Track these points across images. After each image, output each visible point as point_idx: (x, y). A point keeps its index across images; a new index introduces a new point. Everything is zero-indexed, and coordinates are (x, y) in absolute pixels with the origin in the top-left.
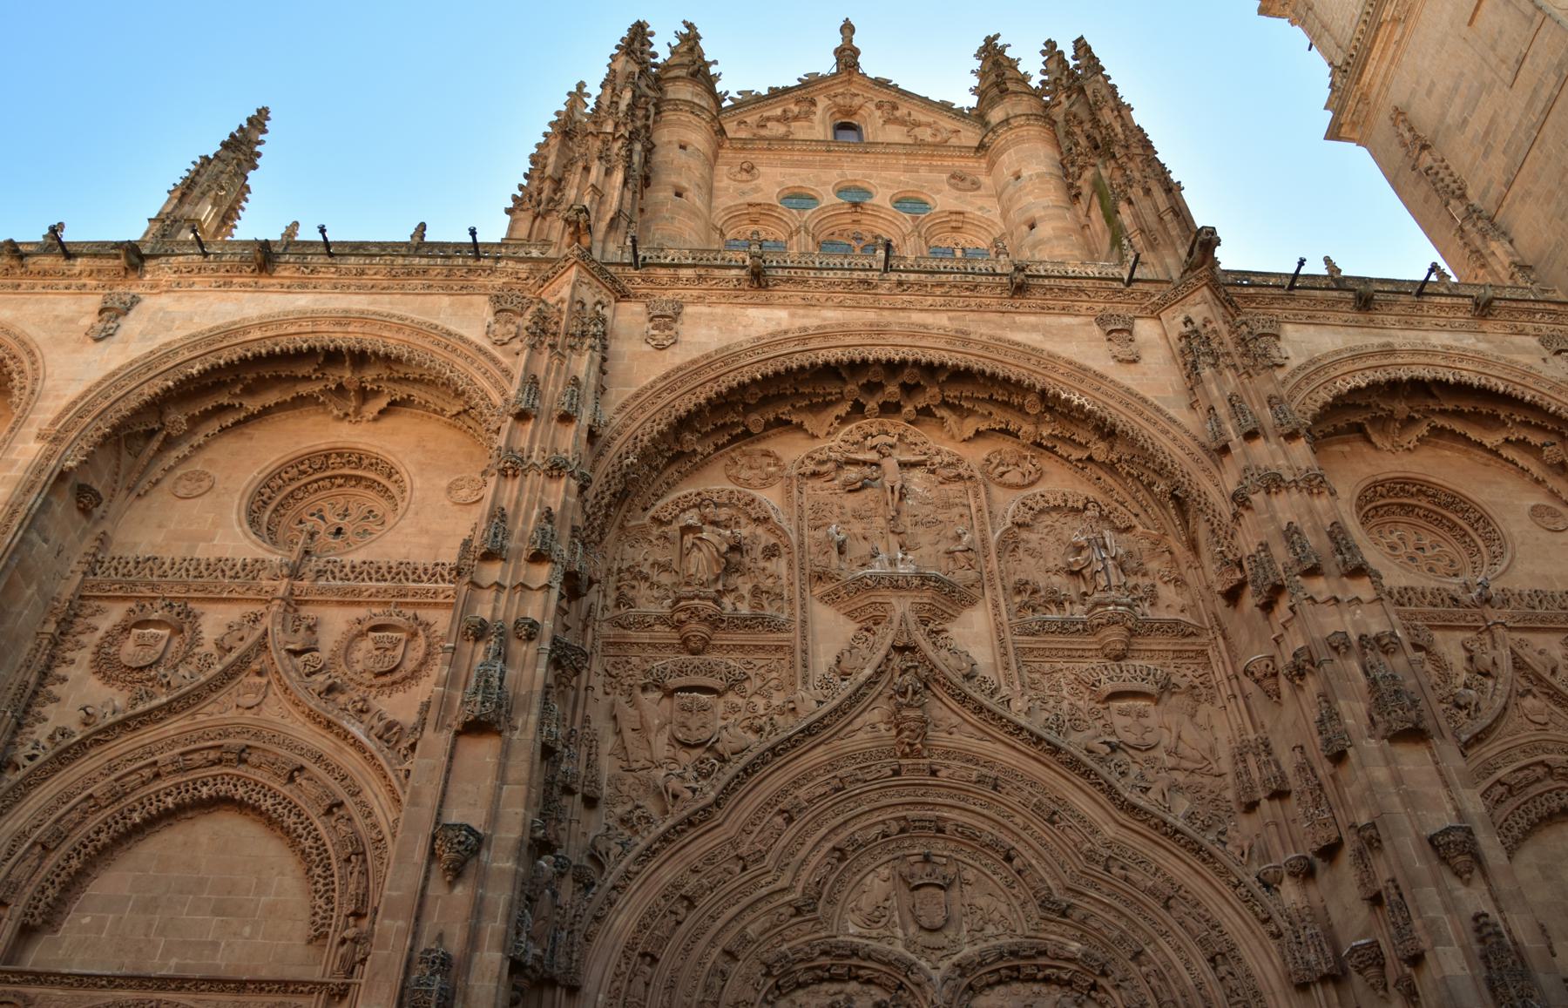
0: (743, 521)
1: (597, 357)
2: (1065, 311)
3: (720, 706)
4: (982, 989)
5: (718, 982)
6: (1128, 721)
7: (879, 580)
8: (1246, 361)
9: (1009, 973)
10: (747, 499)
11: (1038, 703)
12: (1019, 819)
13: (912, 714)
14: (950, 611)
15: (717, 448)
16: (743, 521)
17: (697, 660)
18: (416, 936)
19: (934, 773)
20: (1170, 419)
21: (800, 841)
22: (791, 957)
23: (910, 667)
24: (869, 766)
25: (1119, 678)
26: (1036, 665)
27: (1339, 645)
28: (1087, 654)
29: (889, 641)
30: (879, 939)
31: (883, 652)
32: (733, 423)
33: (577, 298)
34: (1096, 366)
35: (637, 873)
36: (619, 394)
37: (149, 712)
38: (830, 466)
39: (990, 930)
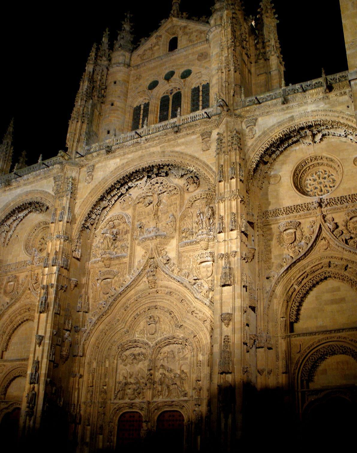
1: (69, 197)
2: (193, 133)
3: (113, 281)
4: (163, 347)
6: (205, 269)
7: (146, 239)
8: (229, 148)
10: (121, 217)
12: (175, 303)
13: (151, 278)
15: (116, 201)
16: (121, 223)
18: (34, 357)
20: (214, 172)
22: (123, 344)
27: (222, 256)
29: (147, 257)
30: (142, 337)
31: (146, 261)
32: (116, 194)
33: (66, 176)
34: (197, 155)
36: (79, 202)
37: (12, 304)
39: (165, 333)
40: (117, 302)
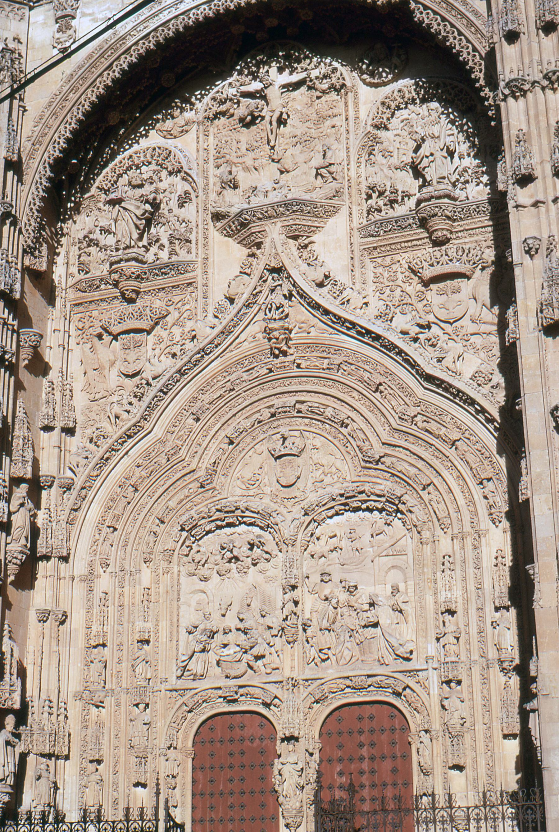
0: (164, 173)
3: (151, 338)
4: (323, 520)
5: (152, 538)
9: (343, 507)
11: (378, 294)
14: (316, 224)
17: (131, 308)
19: (298, 366)
21: (205, 433)
22: (196, 516)
23: (276, 287)
24: (253, 368)
25: (438, 263)
26: (379, 260)
28: (420, 242)
35: (97, 476)
38: (228, 103)
40: (168, 398)
